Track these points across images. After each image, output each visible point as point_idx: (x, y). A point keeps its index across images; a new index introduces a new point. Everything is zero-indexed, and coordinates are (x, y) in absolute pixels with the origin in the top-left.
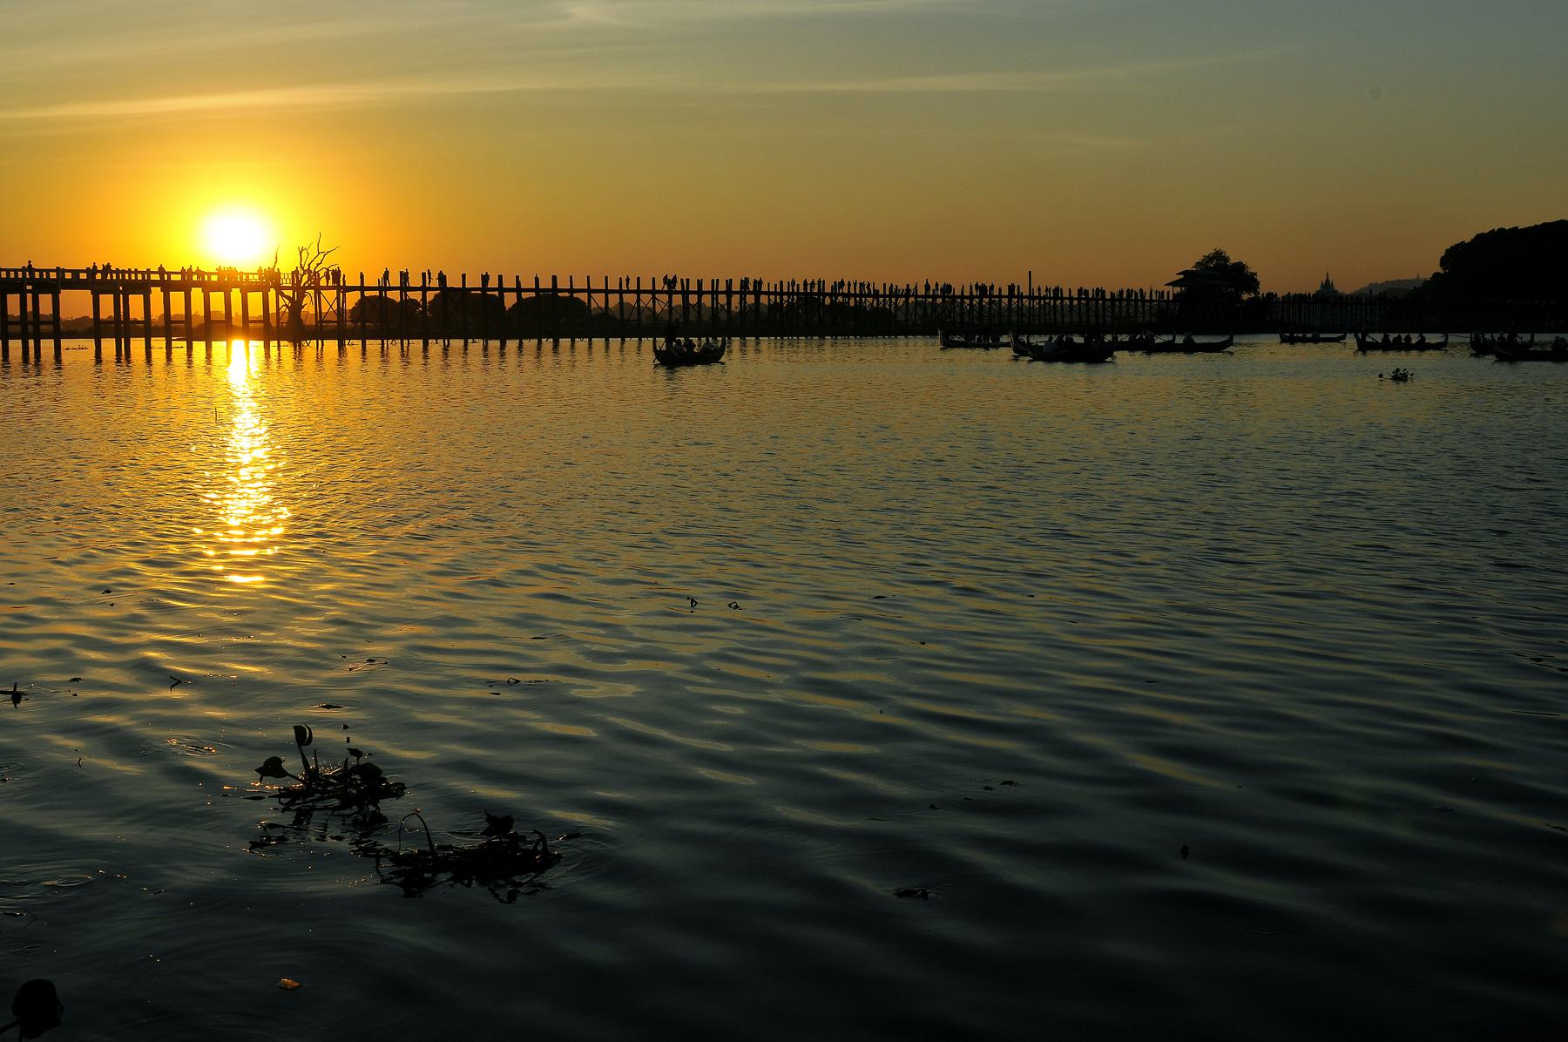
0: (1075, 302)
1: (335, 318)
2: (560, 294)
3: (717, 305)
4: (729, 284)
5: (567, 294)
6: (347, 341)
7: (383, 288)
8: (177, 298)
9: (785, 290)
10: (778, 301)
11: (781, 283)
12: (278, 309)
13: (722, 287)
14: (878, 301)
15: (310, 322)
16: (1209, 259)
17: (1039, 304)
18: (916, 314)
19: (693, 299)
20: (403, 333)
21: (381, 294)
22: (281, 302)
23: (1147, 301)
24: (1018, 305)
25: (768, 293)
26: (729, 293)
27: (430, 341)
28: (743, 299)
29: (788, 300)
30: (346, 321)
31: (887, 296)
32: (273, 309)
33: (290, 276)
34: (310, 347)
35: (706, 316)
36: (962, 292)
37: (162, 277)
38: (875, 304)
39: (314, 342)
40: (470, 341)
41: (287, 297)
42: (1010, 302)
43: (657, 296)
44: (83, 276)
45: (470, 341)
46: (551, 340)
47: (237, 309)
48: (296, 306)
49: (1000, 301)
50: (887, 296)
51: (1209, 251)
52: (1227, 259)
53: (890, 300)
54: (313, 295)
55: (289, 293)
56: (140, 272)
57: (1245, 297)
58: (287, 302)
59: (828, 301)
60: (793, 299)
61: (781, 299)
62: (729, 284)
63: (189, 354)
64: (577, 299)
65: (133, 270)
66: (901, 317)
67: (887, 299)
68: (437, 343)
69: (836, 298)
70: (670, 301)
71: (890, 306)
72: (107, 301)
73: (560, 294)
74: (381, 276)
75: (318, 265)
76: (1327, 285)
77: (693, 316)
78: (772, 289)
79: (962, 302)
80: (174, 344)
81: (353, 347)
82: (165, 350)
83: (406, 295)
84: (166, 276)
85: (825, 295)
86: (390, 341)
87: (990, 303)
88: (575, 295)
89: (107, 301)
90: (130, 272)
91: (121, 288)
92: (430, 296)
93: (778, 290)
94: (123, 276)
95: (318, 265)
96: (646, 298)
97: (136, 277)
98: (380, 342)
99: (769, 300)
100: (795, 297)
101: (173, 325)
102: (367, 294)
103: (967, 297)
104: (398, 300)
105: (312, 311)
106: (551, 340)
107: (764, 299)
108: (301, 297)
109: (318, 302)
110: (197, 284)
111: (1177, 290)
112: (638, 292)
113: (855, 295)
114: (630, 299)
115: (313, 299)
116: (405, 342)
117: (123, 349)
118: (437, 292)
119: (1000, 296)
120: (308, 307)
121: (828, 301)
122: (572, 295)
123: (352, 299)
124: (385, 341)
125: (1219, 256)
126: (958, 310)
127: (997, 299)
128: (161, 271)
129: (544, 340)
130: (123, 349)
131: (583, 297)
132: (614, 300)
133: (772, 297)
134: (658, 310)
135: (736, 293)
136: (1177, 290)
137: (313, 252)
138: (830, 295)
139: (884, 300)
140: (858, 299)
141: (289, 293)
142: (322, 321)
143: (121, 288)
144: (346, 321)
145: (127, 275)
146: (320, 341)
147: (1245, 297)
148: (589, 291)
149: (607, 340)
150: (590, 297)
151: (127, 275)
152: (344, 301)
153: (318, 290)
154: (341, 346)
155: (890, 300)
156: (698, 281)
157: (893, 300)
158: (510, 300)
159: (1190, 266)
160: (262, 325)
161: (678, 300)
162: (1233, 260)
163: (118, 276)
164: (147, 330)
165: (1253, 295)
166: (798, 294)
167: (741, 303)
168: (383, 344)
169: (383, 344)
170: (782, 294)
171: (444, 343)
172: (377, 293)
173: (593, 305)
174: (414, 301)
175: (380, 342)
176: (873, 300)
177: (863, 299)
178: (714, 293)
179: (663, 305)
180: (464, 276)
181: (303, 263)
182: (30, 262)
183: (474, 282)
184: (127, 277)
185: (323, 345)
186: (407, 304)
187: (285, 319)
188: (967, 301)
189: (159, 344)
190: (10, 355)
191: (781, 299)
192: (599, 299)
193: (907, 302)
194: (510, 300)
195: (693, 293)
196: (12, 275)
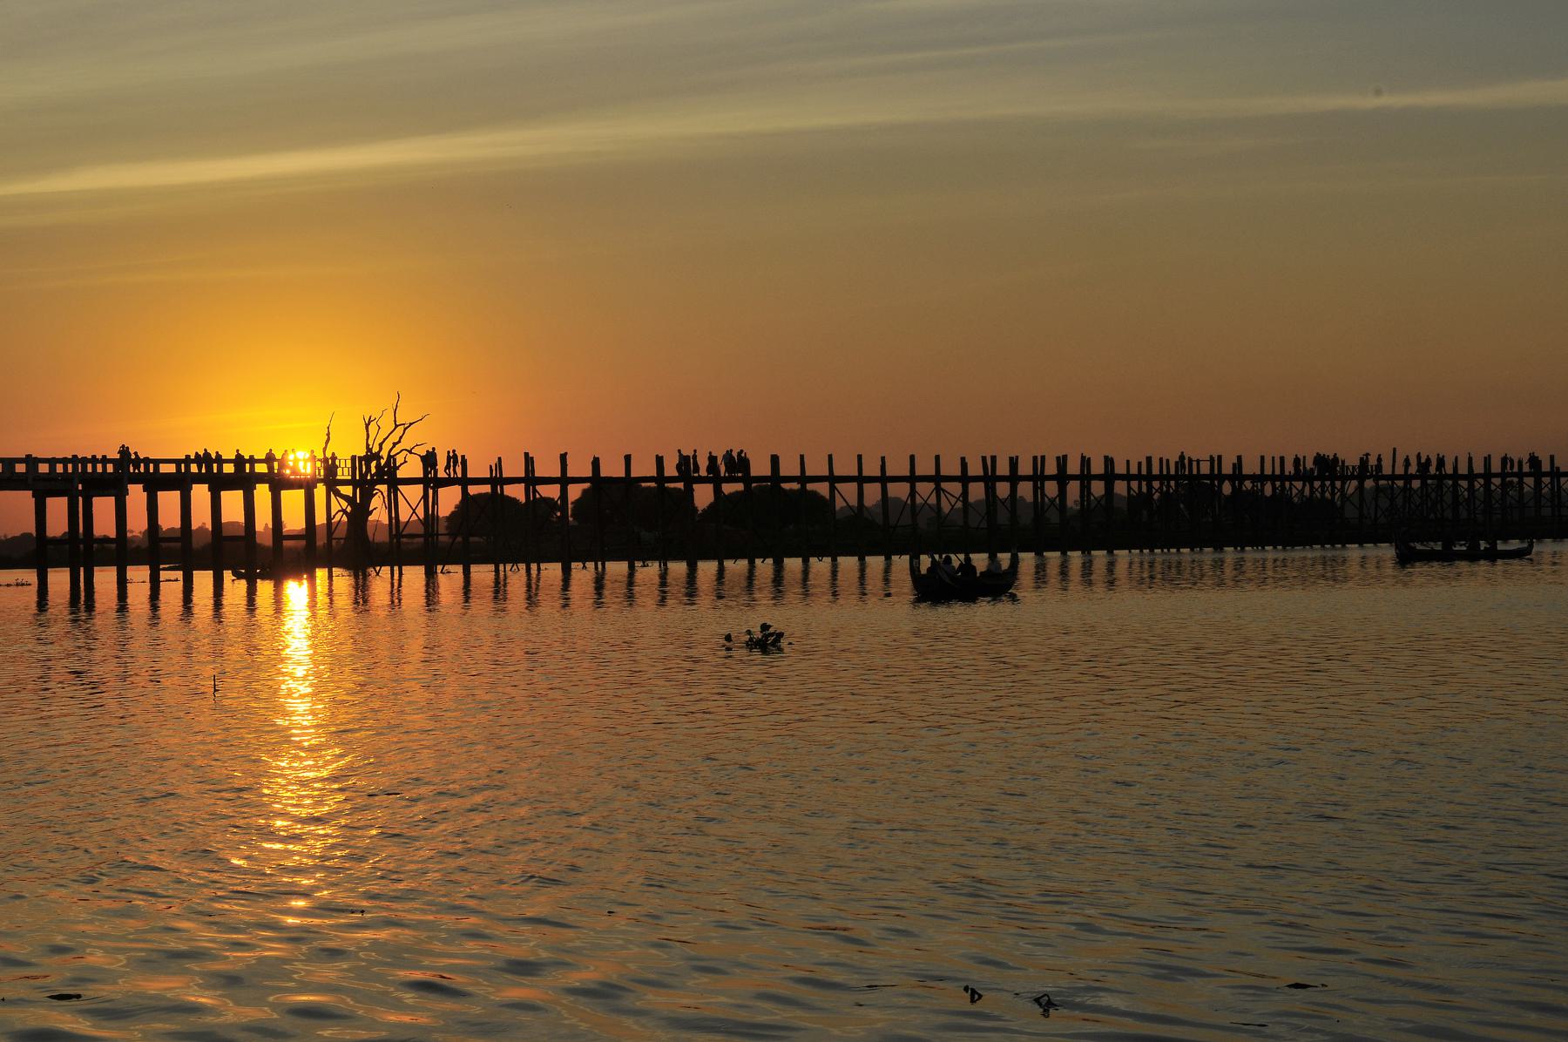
1: (421, 530)
2: (786, 486)
3: (1042, 498)
4: (1062, 462)
5: (795, 486)
6: (439, 568)
7: (497, 480)
8: (232, 503)
9: (1156, 471)
10: (1144, 489)
11: (1149, 459)
12: (329, 517)
13: (1051, 469)
15: (382, 537)
18: (1377, 505)
19: (1003, 489)
20: (532, 554)
21: (495, 489)
22: (335, 507)
25: (1127, 477)
26: (1062, 478)
27: (574, 565)
28: (1085, 489)
29: (1161, 487)
30: (438, 535)
32: (320, 519)
33: (349, 464)
34: (380, 581)
35: (1026, 518)
36: (1455, 468)
37: (271, 468)
38: (1307, 492)
39: (386, 570)
40: (638, 564)
41: (345, 497)
42: (1538, 483)
43: (944, 485)
44: (21, 468)
45: (638, 564)
46: (770, 561)
47: (263, 519)
48: (359, 511)
49: (1521, 483)
53: (1333, 485)
54: (386, 494)
55: (347, 490)
56: (111, 461)
58: (344, 504)
59: (1227, 488)
60: (1169, 486)
61: (1150, 487)
62: (1062, 462)
63: (887, 570)
64: (814, 494)
65: (99, 457)
66: (1351, 512)
67: (1328, 483)
68: (584, 567)
69: (1241, 484)
70: (965, 493)
71: (1333, 494)
72: (57, 507)
73: (786, 486)
75: (395, 444)
77: (1003, 517)
78: (1134, 471)
79: (1456, 485)
80: (164, 575)
81: (450, 579)
82: (148, 585)
83: (535, 491)
84: (151, 466)
85: (1222, 478)
86: (508, 566)
87: (1504, 485)
88: (810, 487)
89: (57, 507)
90: (94, 460)
91: (80, 487)
92: (575, 492)
93: (1144, 472)
94: (84, 468)
95: (395, 444)
96: (925, 489)
97: (104, 468)
98: (492, 567)
99: (1129, 488)
100: (1172, 483)
101: (164, 545)
102: (473, 490)
103: (1463, 477)
104: (522, 499)
106: (770, 561)
107: (1120, 488)
108: (368, 496)
109: (392, 505)
110: (199, 479)
112: (912, 479)
113: (1273, 478)
114: (899, 491)
115: (386, 500)
117: (82, 585)
118: (587, 485)
119: (1521, 475)
120: (378, 512)
121: (1227, 488)
122: (803, 487)
123: (449, 499)
124: (501, 567)
126: (1448, 498)
127: (1515, 480)
128: (270, 459)
129: (758, 561)
130: (82, 585)
131: (823, 489)
132: (872, 493)
133: (1134, 484)
134: (946, 507)
135: (1074, 477)
137: (387, 425)
138: (1231, 478)
139: (1323, 486)
140: (1278, 484)
142: (399, 535)
143: (80, 487)
144: (438, 535)
145: (90, 466)
146: (396, 568)
148: (833, 479)
149: (862, 559)
150: (833, 489)
151: (90, 466)
152: (435, 502)
153: (394, 483)
154: (430, 575)
155: (1333, 485)
156: (1011, 459)
158: (703, 496)
160: (303, 543)
161: (977, 491)
163: (76, 468)
164: (121, 553)
167: (1082, 496)
169: (497, 571)
170: (1150, 478)
171: (596, 568)
172: (486, 489)
173: (839, 503)
175: (492, 567)
176: (1304, 486)
177: (1287, 484)
178: (1038, 478)
179: (953, 500)
180: (628, 458)
181: (370, 442)
182: (695, 451)
183: (644, 468)
184: (90, 469)
186: (539, 506)
187: (341, 533)
188: (1464, 484)
189: (139, 575)
190: (49, 590)
191: (1150, 487)
192: (848, 491)
193: (1361, 487)
194: (703, 496)
195: (1003, 479)
196: (60, 468)
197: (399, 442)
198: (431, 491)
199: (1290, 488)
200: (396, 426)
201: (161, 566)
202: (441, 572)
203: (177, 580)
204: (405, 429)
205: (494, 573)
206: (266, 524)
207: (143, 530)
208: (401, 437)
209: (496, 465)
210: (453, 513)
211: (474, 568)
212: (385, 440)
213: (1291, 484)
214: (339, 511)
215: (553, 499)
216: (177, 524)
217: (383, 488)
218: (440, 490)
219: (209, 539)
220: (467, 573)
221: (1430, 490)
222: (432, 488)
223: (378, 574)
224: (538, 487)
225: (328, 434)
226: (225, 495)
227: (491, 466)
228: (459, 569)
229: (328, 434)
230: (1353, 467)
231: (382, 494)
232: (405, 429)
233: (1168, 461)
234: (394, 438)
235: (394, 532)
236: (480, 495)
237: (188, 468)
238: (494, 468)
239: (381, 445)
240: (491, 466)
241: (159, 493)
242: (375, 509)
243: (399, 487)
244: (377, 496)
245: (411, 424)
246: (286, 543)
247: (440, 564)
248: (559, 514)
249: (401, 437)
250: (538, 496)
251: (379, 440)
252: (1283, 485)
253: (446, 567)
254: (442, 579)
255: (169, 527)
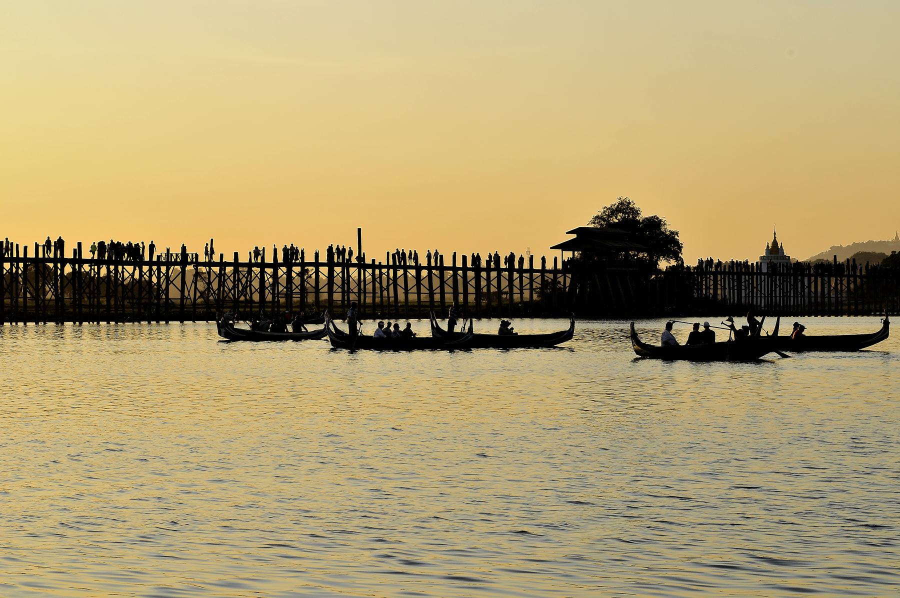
0: (424, 273)
14: (141, 271)
16: (614, 212)
17: (373, 274)
18: (196, 288)
23: (526, 271)
24: (343, 277)
29: (11, 269)
31: (155, 263)
38: (137, 276)
42: (331, 272)
50: (155, 263)
51: (613, 201)
52: (636, 212)
57: (663, 264)
60: (17, 268)
66: (174, 293)
67: (154, 268)
69: (80, 267)
76: (775, 250)
85: (64, 261)
100: (21, 265)
103: (269, 265)
111: (568, 255)
119: (317, 264)
121: (68, 269)
125: (624, 207)
126: (256, 284)
136: (568, 255)
138: (72, 262)
139: (150, 270)
147: (663, 264)
157: (163, 269)
159: (586, 222)
162: (645, 214)
165: (673, 263)
166: (25, 260)
176: (135, 269)
177: (120, 268)
188: (269, 271)
199: (123, 272)
213: (123, 268)
221: (241, 276)
230: (177, 255)
233: (17, 245)
252: (116, 269)
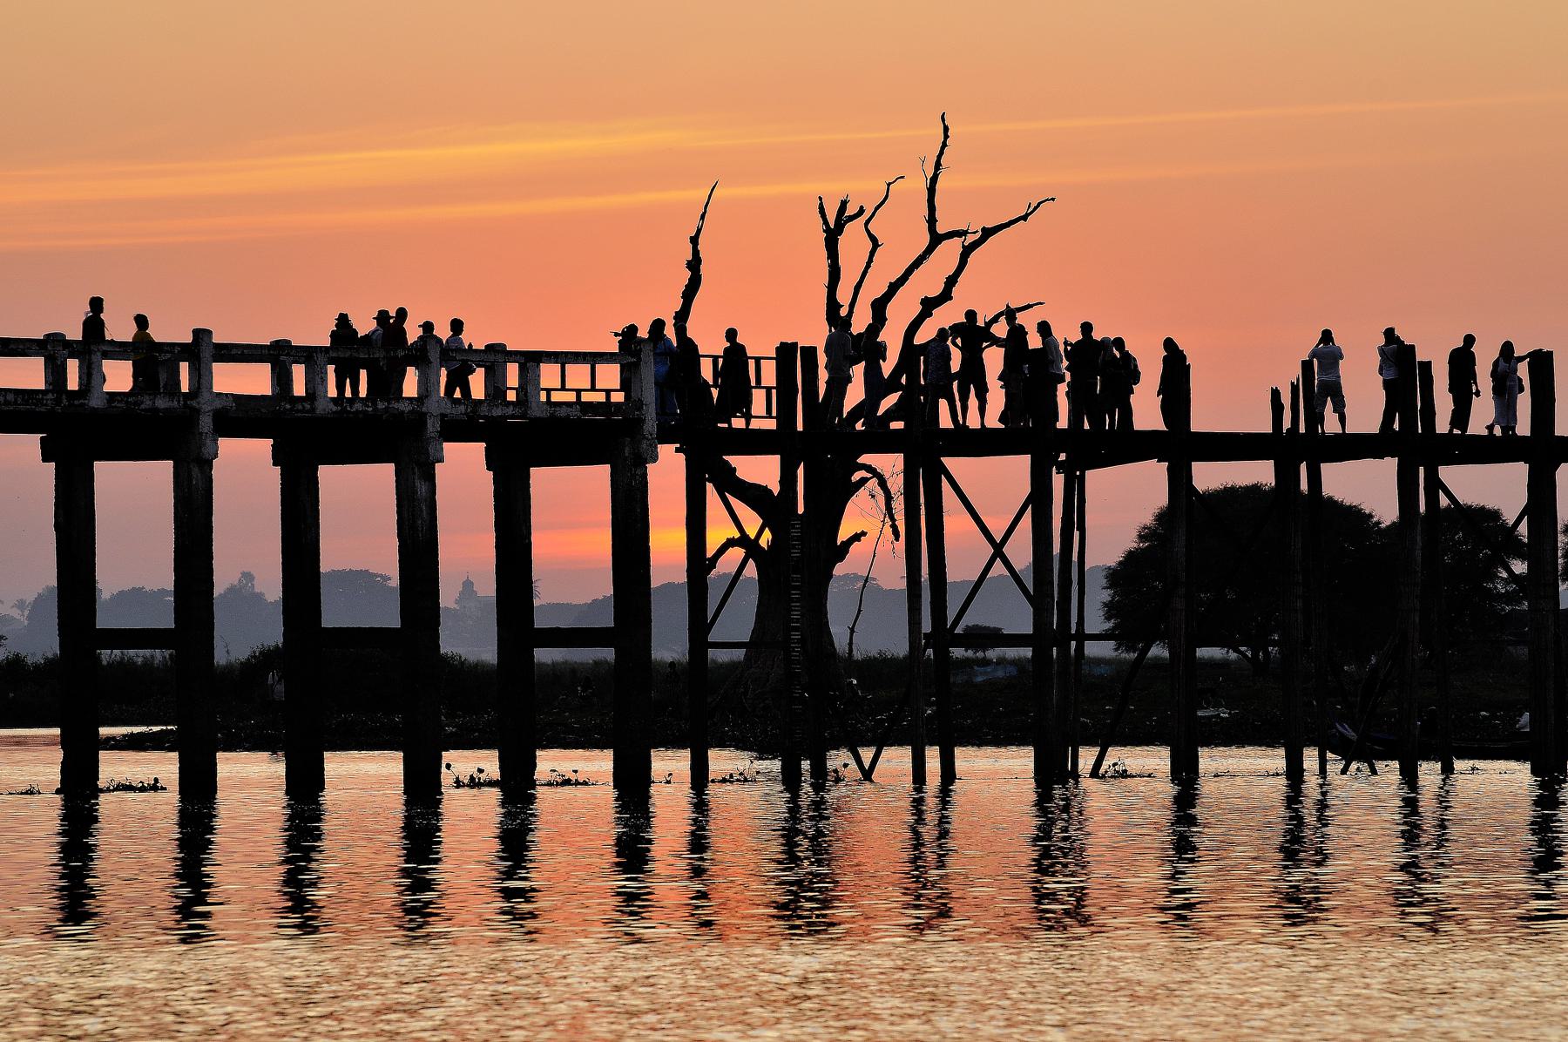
21: (1286, 475)
22: (718, 532)
30: (1082, 637)
39: (896, 760)
41: (754, 495)
54: (897, 484)
58: (752, 522)
74: (1287, 375)
75: (929, 305)
80: (112, 767)
83: (1435, 485)
95: (929, 305)
98: (1275, 760)
102: (1209, 476)
104: (1386, 511)
105: (892, 574)
115: (899, 505)
116: (1429, 772)
141: (762, 470)
142: (943, 636)
168: (1295, 773)
169: (1295, 773)
172: (1261, 473)
174: (1482, 520)
175: (1275, 760)
181: (844, 295)
185: (948, 774)
197: (946, 296)
198: (1058, 481)
200: (936, 239)
201: (104, 731)
202: (1095, 773)
203: (155, 787)
204: (967, 252)
205: (1282, 781)
206: (468, 584)
207: (30, 598)
208: (951, 281)
209: (1295, 388)
210: (1131, 556)
211: (1210, 760)
212: (894, 288)
214: (730, 543)
215: (1495, 515)
216: (160, 574)
217: (891, 464)
218: (1096, 479)
219: (273, 634)
220: (1185, 773)
222: (1061, 467)
223: (867, 775)
224: (1446, 473)
225: (694, 265)
226: (333, 479)
227: (1276, 394)
228: (1156, 760)
229: (694, 265)
231: (883, 483)
232: (967, 252)
234: (928, 281)
235: (927, 627)
236: (1230, 495)
237: (90, 374)
238: (1286, 399)
239: (879, 307)
240: (1276, 394)
241: (99, 466)
242: (857, 537)
243: (946, 461)
244: (862, 493)
245: (987, 233)
246: (544, 655)
247: (1090, 743)
248: (1519, 567)
249: (951, 281)
250: (1444, 501)
251: (874, 288)
253: (1115, 755)
254: (1096, 797)
255: (127, 586)
